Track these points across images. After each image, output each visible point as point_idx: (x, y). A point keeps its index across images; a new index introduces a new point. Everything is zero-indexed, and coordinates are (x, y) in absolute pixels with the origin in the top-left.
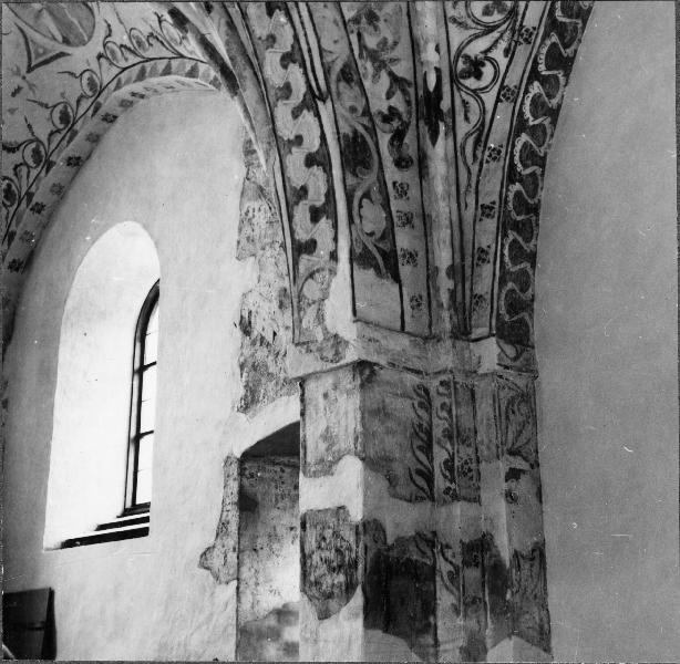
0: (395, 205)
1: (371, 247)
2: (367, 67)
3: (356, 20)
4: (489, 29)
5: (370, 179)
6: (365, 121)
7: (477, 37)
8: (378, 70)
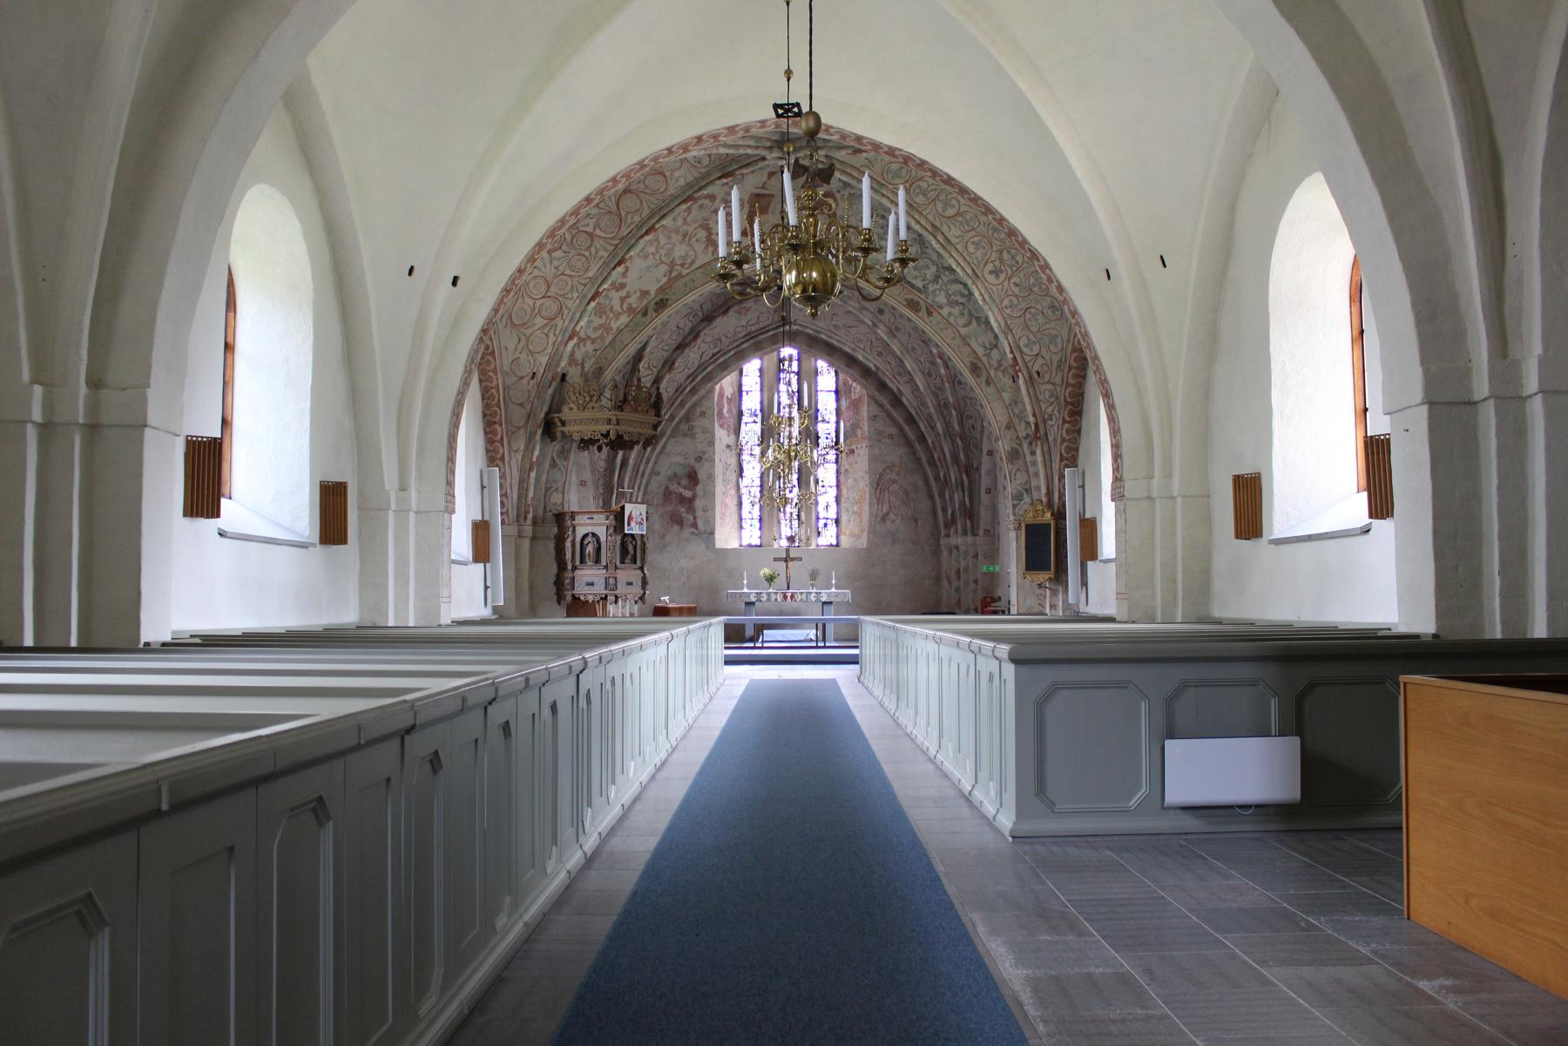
0: (1031, 470)
1: (1022, 490)
2: (1016, 421)
3: (1010, 404)
4: (1052, 404)
5: (1020, 463)
6: (1018, 441)
7: (1048, 407)
8: (1020, 421)
